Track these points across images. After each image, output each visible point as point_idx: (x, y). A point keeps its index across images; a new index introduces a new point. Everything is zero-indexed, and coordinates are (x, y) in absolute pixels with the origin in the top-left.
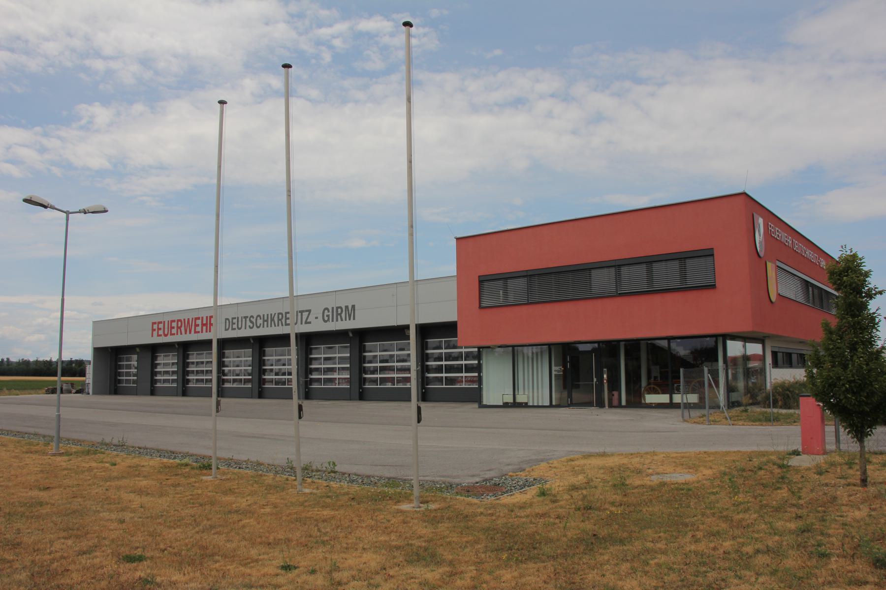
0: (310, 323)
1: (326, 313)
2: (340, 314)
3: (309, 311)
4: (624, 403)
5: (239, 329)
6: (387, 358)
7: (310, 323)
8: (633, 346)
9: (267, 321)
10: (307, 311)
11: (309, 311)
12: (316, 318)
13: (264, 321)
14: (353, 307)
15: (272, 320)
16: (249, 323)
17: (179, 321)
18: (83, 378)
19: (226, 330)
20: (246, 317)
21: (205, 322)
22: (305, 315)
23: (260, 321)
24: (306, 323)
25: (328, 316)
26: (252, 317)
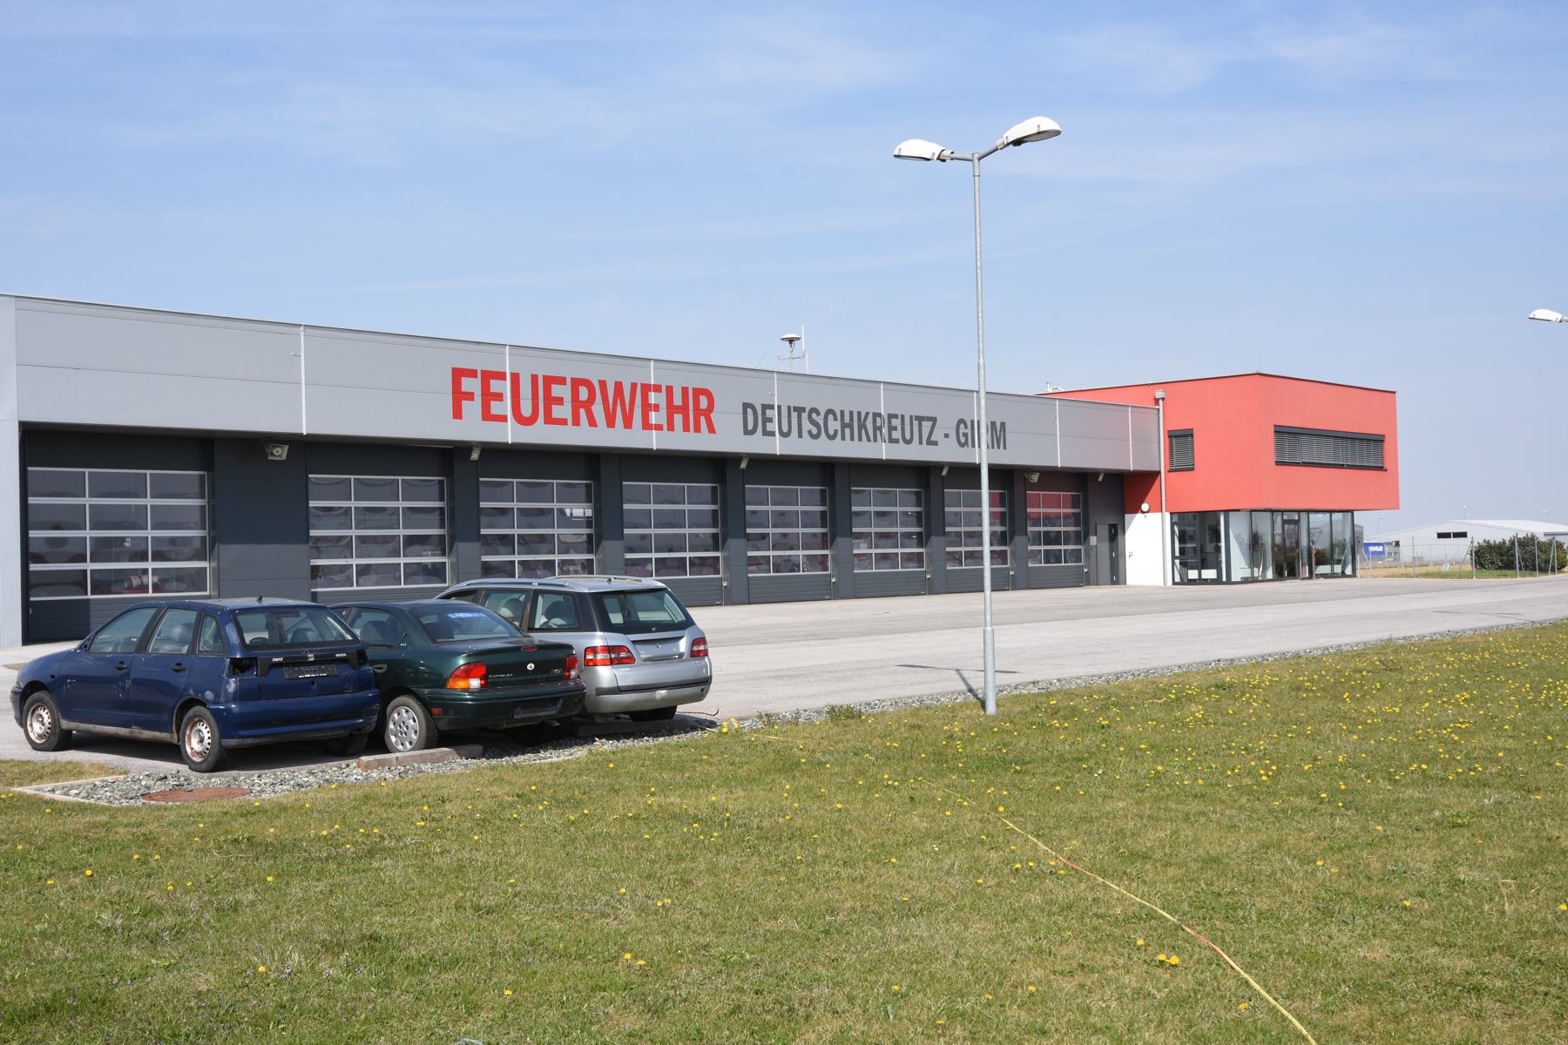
0: (936, 443)
1: (962, 430)
2: (880, 428)
3: (934, 420)
4: (34, 567)
5: (908, 442)
6: (884, 541)
7: (936, 443)
8: (1543, 570)
9: (850, 426)
10: (929, 419)
11: (934, 420)
12: (947, 436)
13: (844, 426)
14: (1003, 425)
15: (862, 426)
16: (807, 426)
17: (577, 383)
18: (65, 724)
19: (747, 432)
20: (800, 410)
21: (678, 401)
22: (927, 425)
23: (834, 425)
24: (931, 443)
25: (965, 435)
26: (814, 410)
